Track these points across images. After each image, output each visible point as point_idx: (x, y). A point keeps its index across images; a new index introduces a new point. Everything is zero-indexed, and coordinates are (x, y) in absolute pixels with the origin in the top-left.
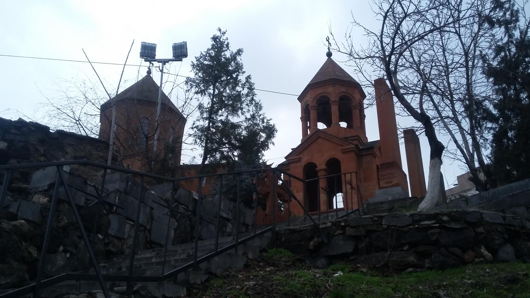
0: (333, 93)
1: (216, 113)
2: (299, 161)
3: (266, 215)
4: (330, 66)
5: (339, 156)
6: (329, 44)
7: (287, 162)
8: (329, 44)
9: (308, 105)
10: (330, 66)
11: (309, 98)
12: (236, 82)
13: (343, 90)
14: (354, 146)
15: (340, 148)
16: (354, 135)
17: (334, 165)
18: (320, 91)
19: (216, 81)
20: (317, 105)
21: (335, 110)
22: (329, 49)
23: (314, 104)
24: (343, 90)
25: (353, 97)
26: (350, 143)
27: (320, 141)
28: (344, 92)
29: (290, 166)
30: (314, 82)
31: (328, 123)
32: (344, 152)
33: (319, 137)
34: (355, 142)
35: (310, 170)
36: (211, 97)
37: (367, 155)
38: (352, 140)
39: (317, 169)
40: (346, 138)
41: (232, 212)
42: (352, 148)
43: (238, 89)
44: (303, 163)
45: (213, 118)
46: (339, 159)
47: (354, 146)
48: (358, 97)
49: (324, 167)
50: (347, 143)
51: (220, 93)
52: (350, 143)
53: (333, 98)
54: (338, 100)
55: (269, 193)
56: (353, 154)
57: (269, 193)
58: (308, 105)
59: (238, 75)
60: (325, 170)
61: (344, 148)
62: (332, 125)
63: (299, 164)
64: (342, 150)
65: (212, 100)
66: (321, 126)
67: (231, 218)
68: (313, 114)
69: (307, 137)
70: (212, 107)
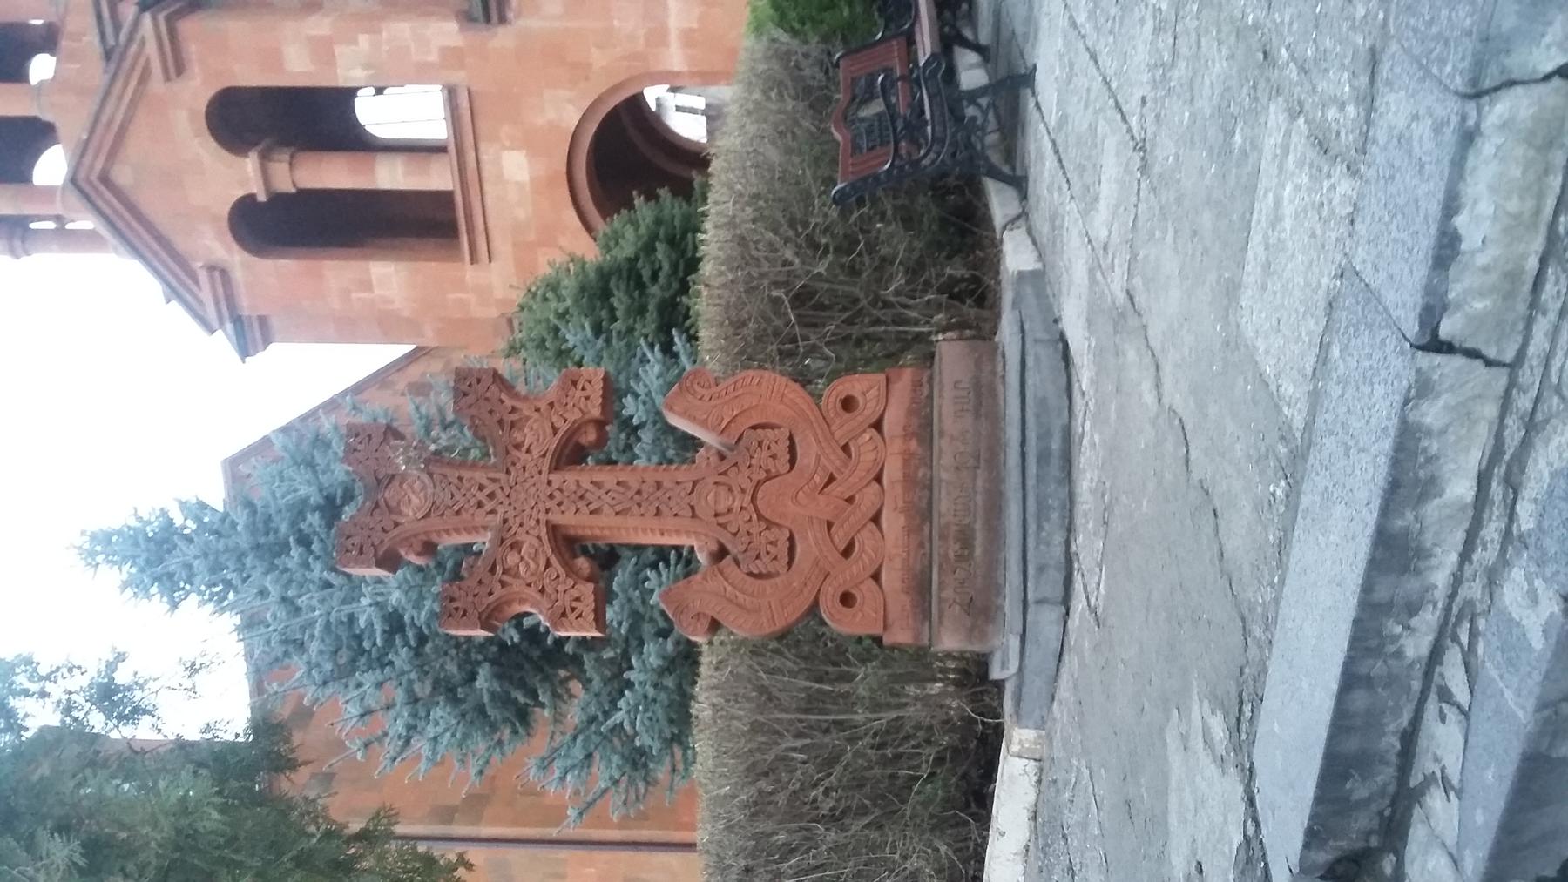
2: (224, 272)
5: (197, 91)
7: (229, 326)
14: (147, 19)
15: (157, 84)
16: (91, 20)
17: (246, 118)
26: (130, 39)
27: (123, 175)
29: (245, 313)
32: (177, 66)
33: (105, 179)
35: (272, 225)
38: (117, 27)
39: (262, 198)
40: (108, 55)
44: (236, 259)
46: (212, 92)
47: (147, 19)
49: (250, 164)
50: (133, 49)
52: (130, 39)
55: (553, 529)
57: (553, 529)
60: (265, 157)
62: (47, 117)
63: (238, 275)
64: (168, 79)
66: (51, 167)
69: (104, 232)
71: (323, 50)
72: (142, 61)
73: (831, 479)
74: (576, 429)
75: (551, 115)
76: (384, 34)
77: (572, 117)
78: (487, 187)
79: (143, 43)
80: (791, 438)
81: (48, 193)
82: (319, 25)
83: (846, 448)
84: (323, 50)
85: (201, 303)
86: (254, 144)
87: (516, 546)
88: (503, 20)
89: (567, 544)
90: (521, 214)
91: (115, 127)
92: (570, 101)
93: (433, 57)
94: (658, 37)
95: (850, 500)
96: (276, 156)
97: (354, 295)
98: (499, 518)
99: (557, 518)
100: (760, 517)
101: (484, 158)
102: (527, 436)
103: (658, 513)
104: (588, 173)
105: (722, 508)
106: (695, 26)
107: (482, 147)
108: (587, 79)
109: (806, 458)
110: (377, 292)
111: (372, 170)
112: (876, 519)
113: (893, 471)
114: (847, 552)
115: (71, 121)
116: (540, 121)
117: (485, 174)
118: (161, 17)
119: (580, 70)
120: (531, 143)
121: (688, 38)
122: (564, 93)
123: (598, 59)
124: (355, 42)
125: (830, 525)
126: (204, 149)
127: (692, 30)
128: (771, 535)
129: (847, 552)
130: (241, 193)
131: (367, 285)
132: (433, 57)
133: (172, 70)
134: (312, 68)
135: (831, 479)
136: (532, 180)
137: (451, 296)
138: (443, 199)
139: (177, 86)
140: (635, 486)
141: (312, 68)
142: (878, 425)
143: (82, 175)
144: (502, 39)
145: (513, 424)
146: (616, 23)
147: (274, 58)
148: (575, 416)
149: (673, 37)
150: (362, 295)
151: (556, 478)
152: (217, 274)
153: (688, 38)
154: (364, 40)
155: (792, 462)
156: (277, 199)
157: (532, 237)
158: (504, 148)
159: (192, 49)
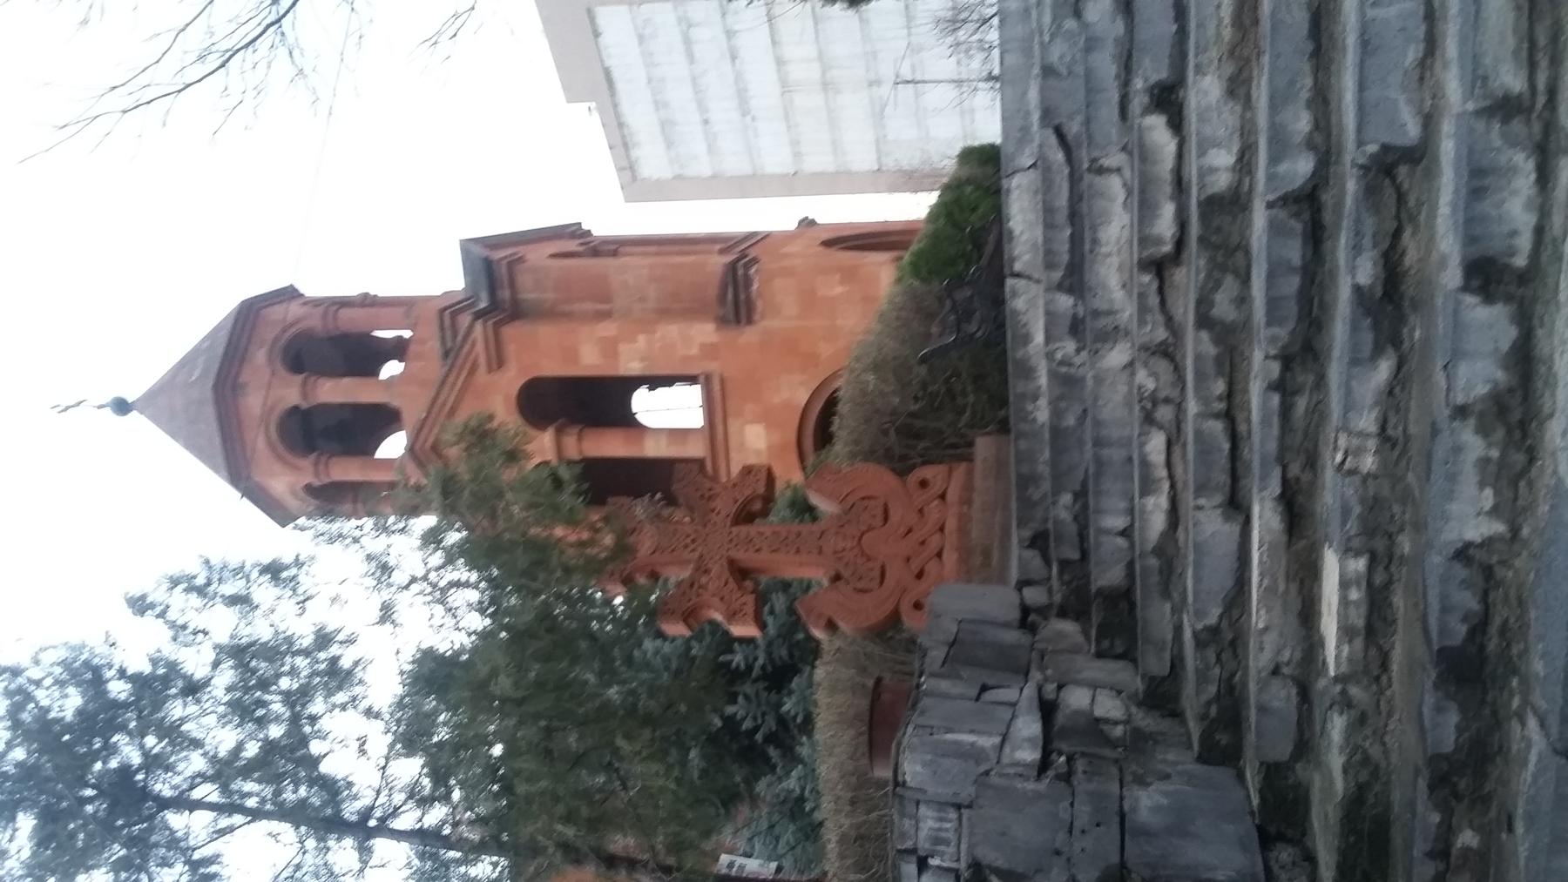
0: (272, 392)
1: (332, 789)
3: (837, 578)
4: (161, 404)
9: (310, 490)
10: (161, 404)
11: (283, 482)
12: (157, 685)
13: (260, 356)
15: (482, 375)
16: (435, 328)
18: (259, 442)
19: (145, 794)
20: (313, 456)
21: (336, 391)
23: (306, 463)
24: (260, 356)
25: (292, 325)
30: (220, 460)
31: (382, 419)
32: (498, 361)
34: (465, 320)
36: (238, 819)
40: (446, 354)
41: (984, 688)
43: (196, 662)
45: (366, 814)
46: (522, 382)
47: (479, 326)
48: (295, 310)
50: (465, 350)
51: (224, 770)
53: (290, 393)
54: (299, 378)
55: (732, 563)
56: (508, 331)
57: (732, 563)
58: (310, 490)
59: (122, 673)
60: (559, 432)
61: (482, 360)
62: (395, 402)
64: (490, 371)
65: (256, 815)
66: (393, 446)
67: (1030, 690)
68: (346, 470)
70: (295, 814)
71: (610, 348)
72: (472, 357)
73: (910, 531)
74: (749, 501)
76: (658, 335)
77: (802, 397)
79: (473, 345)
80: (886, 505)
81: (387, 463)
82: (608, 329)
83: (921, 511)
86: (550, 424)
87: (707, 571)
88: (750, 321)
89: (741, 573)
91: (447, 408)
93: (694, 351)
95: (923, 543)
96: (569, 430)
98: (697, 554)
99: (734, 554)
100: (863, 554)
102: (718, 504)
103: (798, 551)
104: (815, 436)
105: (839, 548)
107: (730, 421)
109: (895, 517)
112: (939, 555)
113: (951, 524)
114: (920, 575)
115: (412, 411)
116: (776, 400)
118: (490, 323)
120: (768, 418)
123: (825, 350)
125: (908, 560)
128: (870, 564)
129: (920, 575)
132: (694, 351)
133: (495, 366)
135: (910, 531)
136: (769, 448)
140: (784, 534)
142: (943, 496)
143: (417, 447)
144: (749, 336)
145: (710, 498)
147: (572, 355)
148: (748, 492)
151: (735, 530)
155: (886, 519)
159: (511, 349)
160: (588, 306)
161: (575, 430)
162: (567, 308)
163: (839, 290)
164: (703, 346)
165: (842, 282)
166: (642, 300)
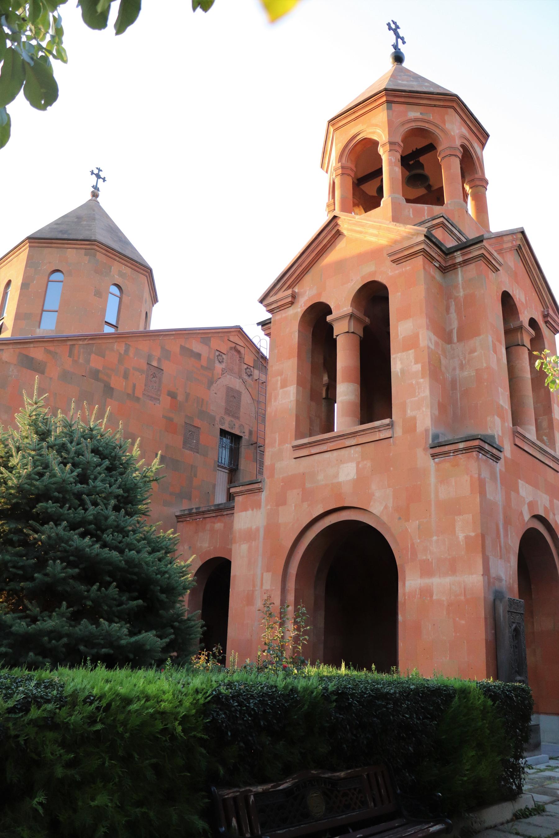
2: (292, 303)
5: (386, 274)
6: (398, 36)
8: (398, 36)
22: (395, 46)
24: (414, 113)
25: (443, 130)
28: (416, 120)
37: (465, 262)
39: (329, 318)
42: (418, 244)
46: (384, 282)
56: (420, 260)
60: (352, 316)
64: (390, 255)
75: (377, 494)
76: (422, 380)
77: (376, 508)
78: (335, 453)
84: (411, 343)
85: (276, 294)
90: (320, 477)
92: (386, 507)
93: (410, 413)
94: (427, 570)
97: (279, 378)
101: (352, 450)
106: (435, 597)
107: (359, 448)
108: (400, 518)
110: (281, 390)
111: (343, 382)
116: (374, 487)
117: (343, 451)
118: (423, 246)
119: (404, 513)
120: (361, 481)
121: (426, 592)
122: (390, 505)
123: (412, 526)
124: (416, 362)
126: (355, 283)
127: (431, 596)
130: (332, 307)
131: (284, 386)
132: (410, 413)
134: (400, 337)
136: (339, 484)
137: (277, 436)
138: (330, 428)
139: (388, 262)
141: (400, 337)
144: (423, 459)
146: (435, 538)
147: (405, 315)
149: (427, 581)
150: (279, 382)
152: (290, 299)
153: (426, 592)
154: (418, 367)
156: (330, 328)
157: (308, 485)
158: (358, 464)
159: (407, 267)
160: (455, 325)
161: (362, 335)
162: (453, 309)
163: (461, 536)
164: (414, 419)
165: (467, 537)
166: (462, 367)
